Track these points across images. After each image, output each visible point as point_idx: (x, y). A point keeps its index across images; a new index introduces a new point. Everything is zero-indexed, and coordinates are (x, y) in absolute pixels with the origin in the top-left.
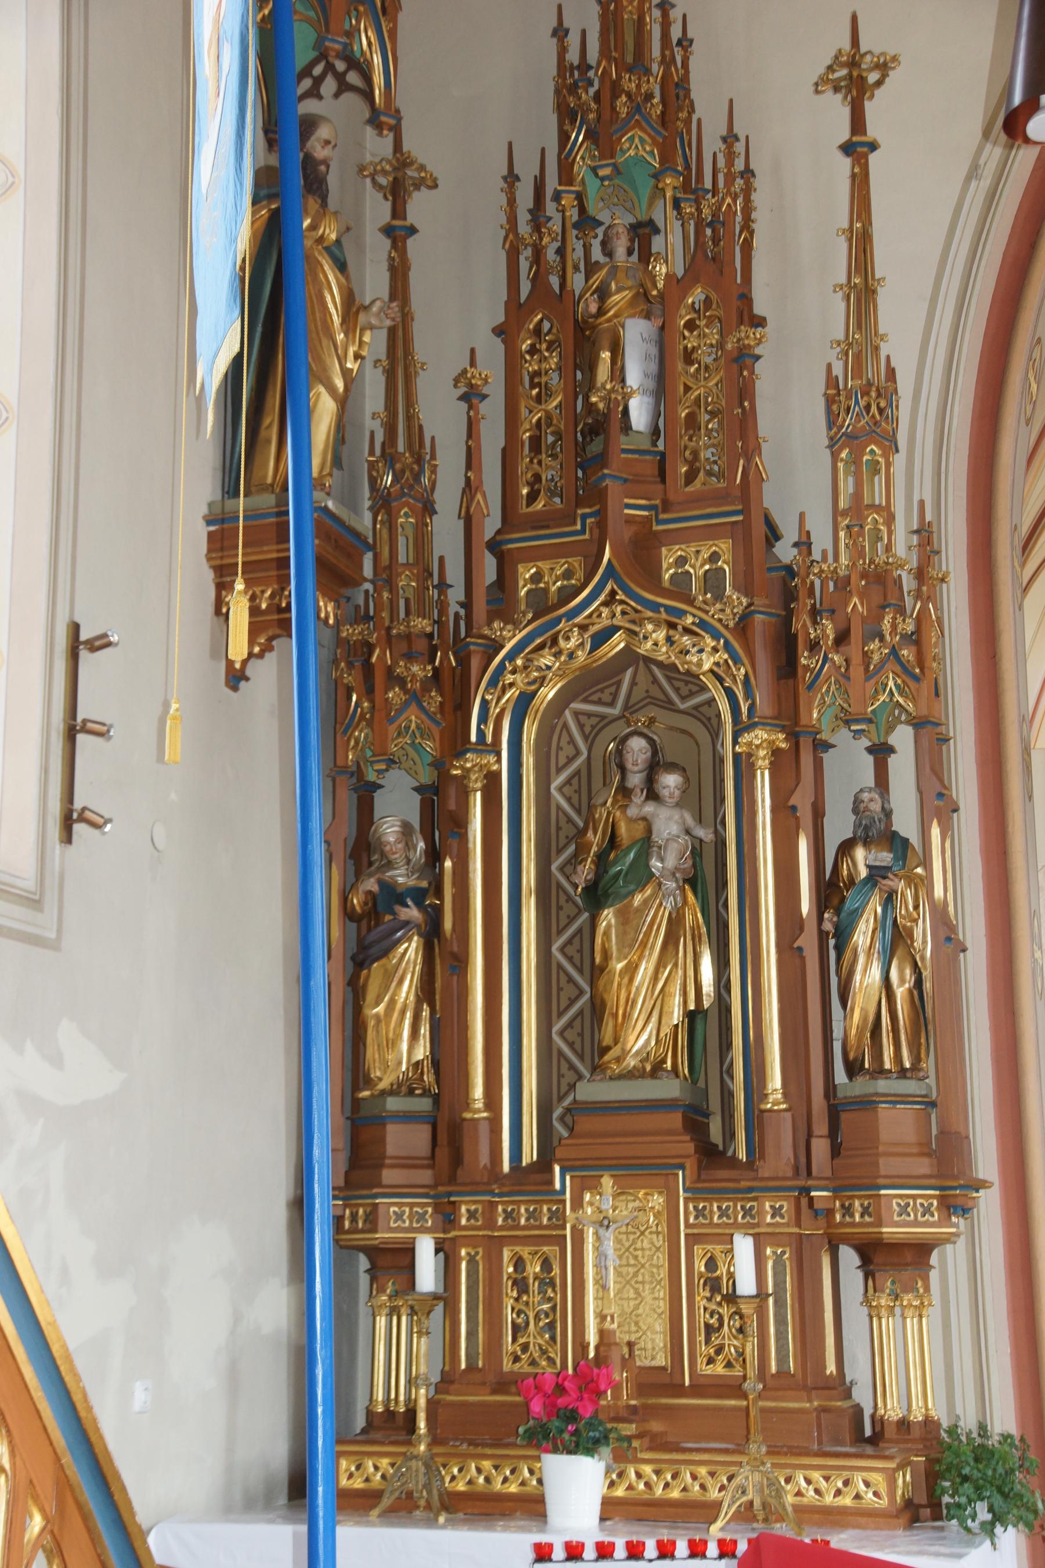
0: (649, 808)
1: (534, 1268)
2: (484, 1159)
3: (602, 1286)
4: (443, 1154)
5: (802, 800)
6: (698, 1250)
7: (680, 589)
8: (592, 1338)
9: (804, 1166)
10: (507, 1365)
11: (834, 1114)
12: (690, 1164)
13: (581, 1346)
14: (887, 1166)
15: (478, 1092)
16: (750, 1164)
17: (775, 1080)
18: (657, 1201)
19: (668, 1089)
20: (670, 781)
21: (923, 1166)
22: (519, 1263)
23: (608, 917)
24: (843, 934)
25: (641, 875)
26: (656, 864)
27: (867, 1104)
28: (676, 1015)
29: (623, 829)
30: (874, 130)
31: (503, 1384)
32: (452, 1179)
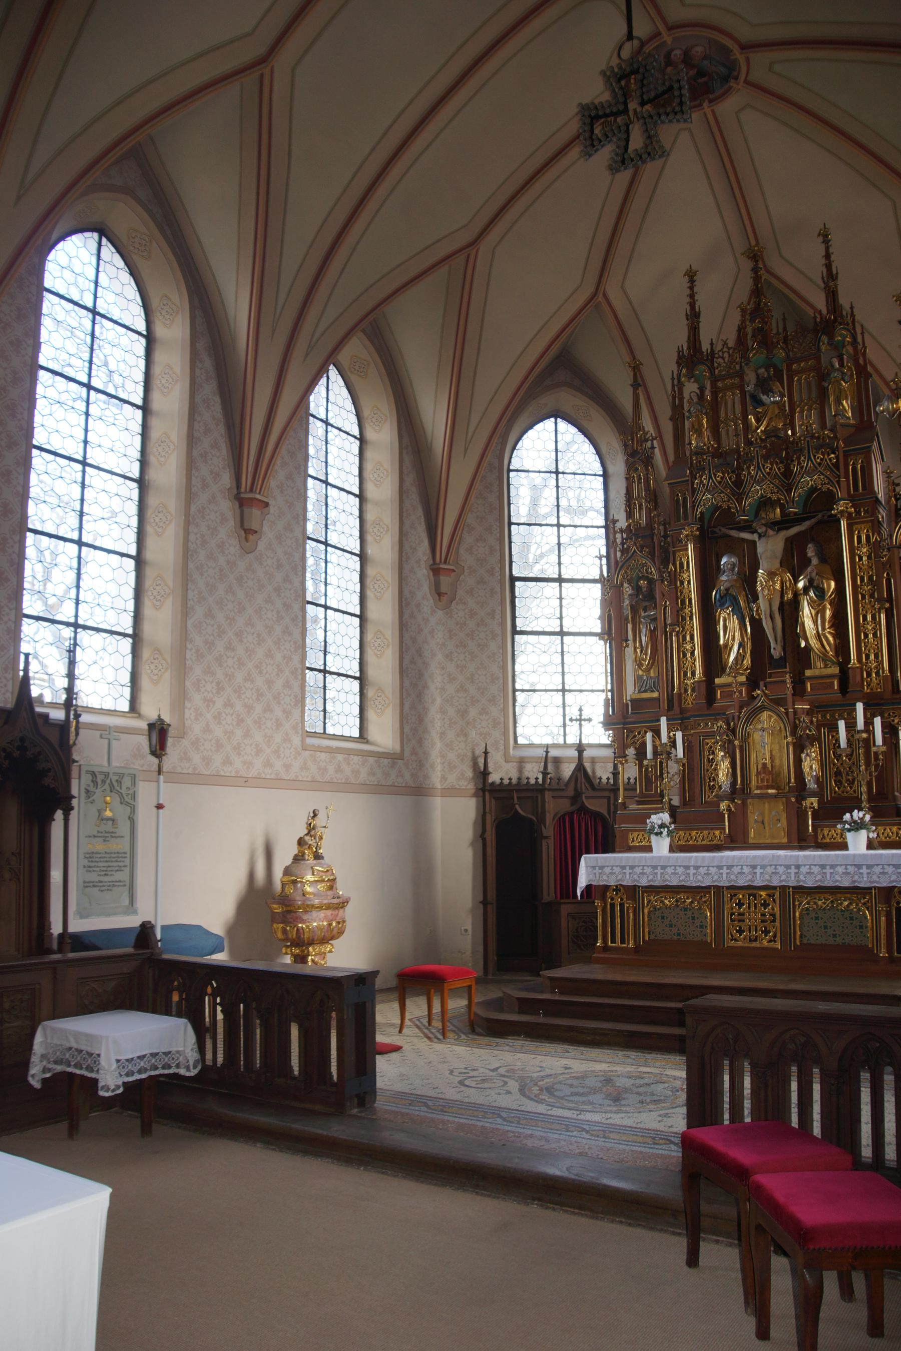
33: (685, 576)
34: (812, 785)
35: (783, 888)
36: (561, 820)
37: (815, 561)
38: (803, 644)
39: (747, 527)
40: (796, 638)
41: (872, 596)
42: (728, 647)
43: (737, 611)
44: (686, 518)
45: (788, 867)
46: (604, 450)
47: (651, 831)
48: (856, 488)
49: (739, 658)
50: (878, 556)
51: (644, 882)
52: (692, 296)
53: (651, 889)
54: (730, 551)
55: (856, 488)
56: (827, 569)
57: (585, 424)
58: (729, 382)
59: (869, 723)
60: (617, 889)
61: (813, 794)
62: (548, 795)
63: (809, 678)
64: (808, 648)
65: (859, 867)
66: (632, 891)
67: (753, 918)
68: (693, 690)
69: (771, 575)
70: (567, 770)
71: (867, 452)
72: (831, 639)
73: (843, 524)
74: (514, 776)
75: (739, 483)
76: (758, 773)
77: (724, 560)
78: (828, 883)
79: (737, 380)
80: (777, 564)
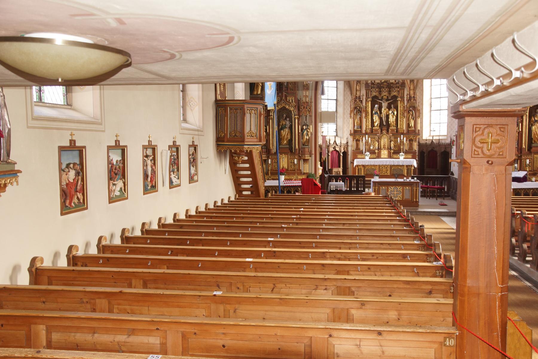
0: (286, 121)
1: (276, 161)
2: (272, 152)
4: (268, 152)
6: (290, 160)
7: (289, 102)
10: (274, 169)
12: (290, 153)
14: (306, 153)
15: (271, 146)
17: (297, 146)
20: (288, 119)
22: (275, 161)
23: (282, 131)
24: (303, 133)
25: (286, 128)
28: (288, 140)
31: (274, 170)
32: (269, 154)
34: (392, 148)
35: (390, 165)
36: (332, 152)
37: (393, 108)
38: (390, 123)
39: (381, 100)
41: (402, 115)
42: (376, 122)
43: (378, 115)
44: (368, 96)
45: (392, 162)
47: (366, 155)
48: (401, 96)
49: (378, 124)
50: (404, 108)
53: (368, 165)
54: (377, 104)
55: (401, 96)
59: (403, 138)
60: (360, 166)
61: (393, 150)
62: (330, 147)
63: (391, 129)
64: (391, 124)
65: (403, 162)
66: (363, 166)
67: (384, 170)
68: (368, 129)
69: (385, 110)
71: (404, 89)
72: (395, 122)
73: (399, 102)
75: (380, 91)
76: (383, 146)
77: (376, 106)
80: (386, 108)
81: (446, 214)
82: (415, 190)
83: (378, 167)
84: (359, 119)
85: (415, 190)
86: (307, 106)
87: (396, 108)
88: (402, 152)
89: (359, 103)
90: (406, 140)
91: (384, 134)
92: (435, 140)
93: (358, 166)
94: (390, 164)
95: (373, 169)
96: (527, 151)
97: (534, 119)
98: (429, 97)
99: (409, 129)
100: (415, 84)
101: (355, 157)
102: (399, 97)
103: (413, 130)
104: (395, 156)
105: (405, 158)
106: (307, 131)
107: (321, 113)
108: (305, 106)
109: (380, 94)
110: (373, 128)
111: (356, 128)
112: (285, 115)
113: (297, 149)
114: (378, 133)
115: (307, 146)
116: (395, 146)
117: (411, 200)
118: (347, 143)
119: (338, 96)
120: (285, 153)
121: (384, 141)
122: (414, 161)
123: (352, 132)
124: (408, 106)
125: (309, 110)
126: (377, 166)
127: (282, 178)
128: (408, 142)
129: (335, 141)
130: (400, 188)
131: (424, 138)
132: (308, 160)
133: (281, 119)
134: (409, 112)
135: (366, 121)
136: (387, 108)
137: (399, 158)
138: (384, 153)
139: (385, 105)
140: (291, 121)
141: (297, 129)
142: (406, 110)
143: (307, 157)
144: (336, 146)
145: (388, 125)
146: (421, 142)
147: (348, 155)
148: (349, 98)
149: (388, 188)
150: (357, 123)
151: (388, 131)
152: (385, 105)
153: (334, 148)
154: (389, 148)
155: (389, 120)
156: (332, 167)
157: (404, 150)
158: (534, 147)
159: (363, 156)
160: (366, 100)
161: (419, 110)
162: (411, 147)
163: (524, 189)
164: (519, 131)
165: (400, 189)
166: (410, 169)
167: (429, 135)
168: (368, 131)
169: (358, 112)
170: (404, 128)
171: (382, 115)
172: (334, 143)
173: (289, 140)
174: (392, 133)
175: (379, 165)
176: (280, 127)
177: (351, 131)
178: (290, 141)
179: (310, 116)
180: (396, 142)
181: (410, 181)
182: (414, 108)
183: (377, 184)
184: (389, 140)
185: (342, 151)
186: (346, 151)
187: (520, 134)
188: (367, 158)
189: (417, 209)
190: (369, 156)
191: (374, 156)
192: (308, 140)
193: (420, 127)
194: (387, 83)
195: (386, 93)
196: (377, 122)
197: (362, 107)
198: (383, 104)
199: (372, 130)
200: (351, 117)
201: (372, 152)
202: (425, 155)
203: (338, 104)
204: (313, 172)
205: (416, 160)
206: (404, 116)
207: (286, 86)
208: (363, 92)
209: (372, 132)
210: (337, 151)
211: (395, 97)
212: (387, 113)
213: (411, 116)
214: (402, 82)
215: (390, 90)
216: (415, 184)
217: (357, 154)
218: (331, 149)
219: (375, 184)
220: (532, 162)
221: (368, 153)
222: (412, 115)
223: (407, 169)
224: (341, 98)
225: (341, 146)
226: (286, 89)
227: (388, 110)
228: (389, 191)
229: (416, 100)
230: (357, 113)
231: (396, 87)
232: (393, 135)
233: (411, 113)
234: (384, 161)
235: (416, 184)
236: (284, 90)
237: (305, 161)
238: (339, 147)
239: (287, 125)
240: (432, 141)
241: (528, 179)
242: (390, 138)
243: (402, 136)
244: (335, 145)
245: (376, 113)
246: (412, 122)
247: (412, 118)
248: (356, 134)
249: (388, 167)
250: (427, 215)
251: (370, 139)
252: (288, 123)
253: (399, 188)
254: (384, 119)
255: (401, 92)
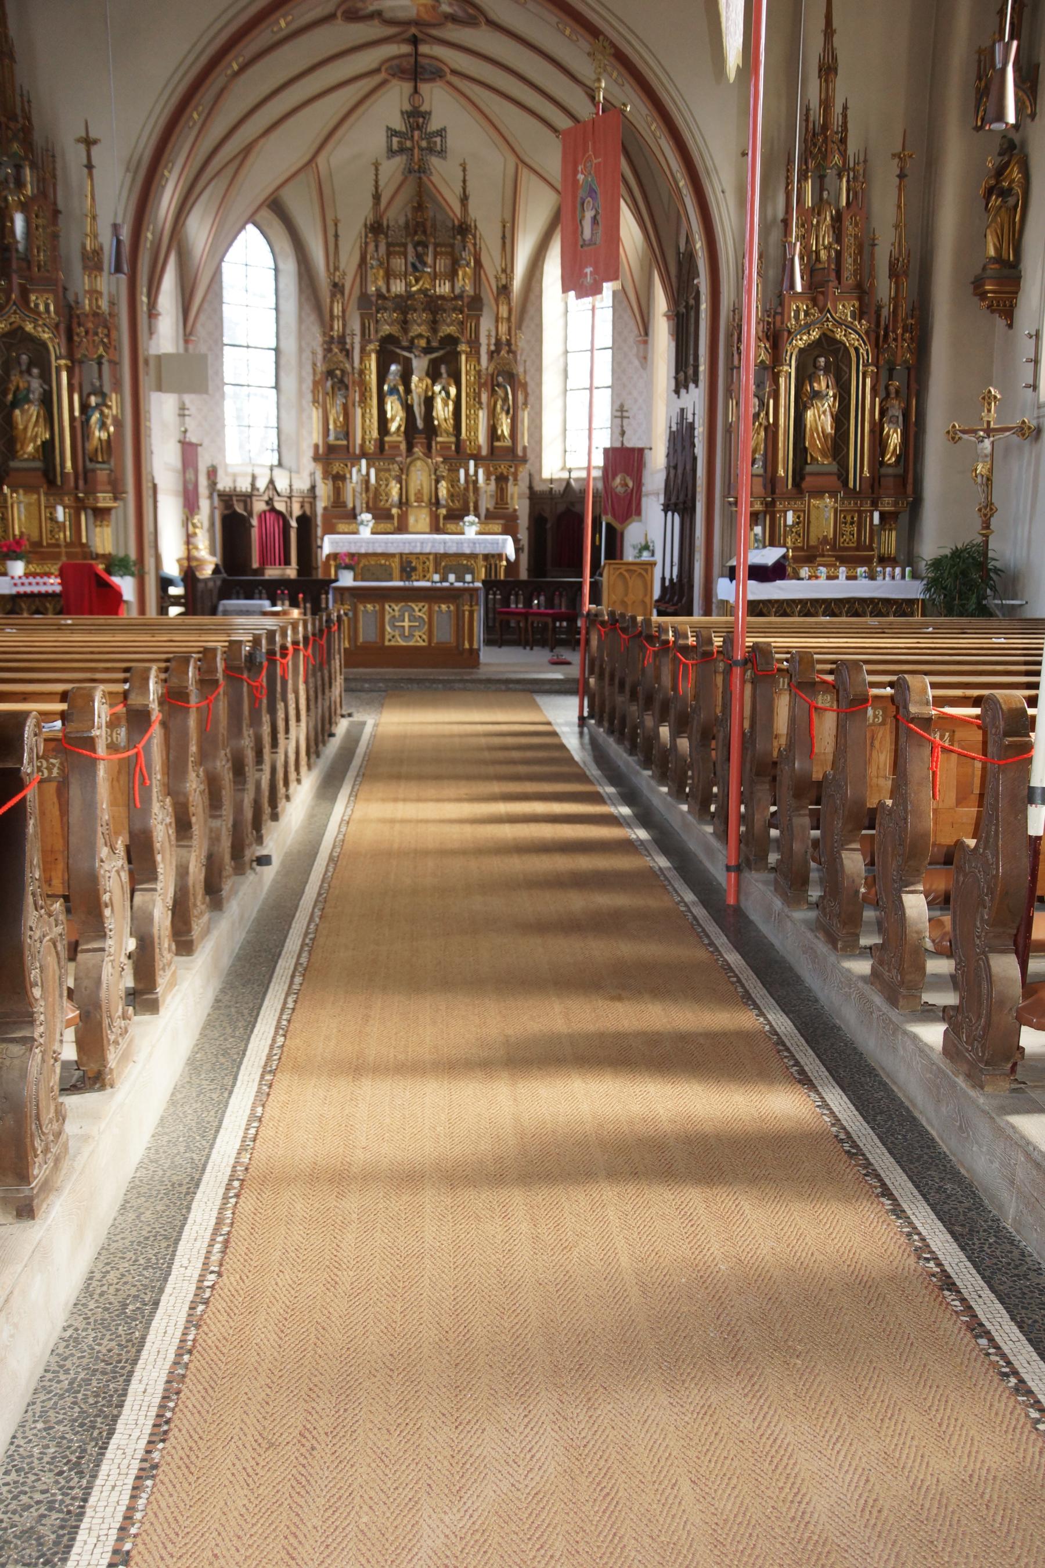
0: (29, 379)
3: (19, 519)
5: (76, 382)
8: (17, 532)
9: (77, 487)
11: (86, 472)
12: (45, 486)
13: (14, 536)
14: (99, 488)
16: (61, 487)
17: (69, 464)
18: (35, 497)
19: (38, 464)
20: (35, 371)
21: (109, 488)
23: (17, 412)
24: (88, 420)
26: (31, 396)
27: (94, 471)
29: (21, 385)
30: (94, 162)
33: (367, 372)
34: (443, 502)
35: (436, 555)
36: (262, 516)
37: (445, 375)
38: (436, 423)
39: (409, 349)
40: (432, 419)
42: (393, 419)
43: (400, 399)
46: (277, 250)
47: (362, 523)
49: (400, 426)
50: (480, 378)
51: (363, 551)
52: (377, 181)
53: (366, 555)
54: (397, 362)
56: (452, 382)
57: (265, 228)
58: (397, 249)
61: (444, 507)
62: (254, 498)
64: (439, 425)
65: (474, 543)
69: (421, 380)
70: (262, 484)
72: (452, 421)
73: (463, 357)
74: (232, 486)
75: (405, 322)
78: (460, 551)
79: (402, 249)
80: (424, 374)
81: (557, 687)
82: (467, 613)
83: (397, 559)
84: (340, 409)
85: (467, 613)
86: (97, 327)
87: (456, 377)
88: (472, 513)
89: (341, 357)
90: (488, 479)
91: (416, 456)
92: (577, 480)
93: (334, 556)
94: (434, 551)
95: (381, 565)
96: (790, 486)
97: (812, 387)
98: (560, 349)
99: (497, 444)
100: (514, 304)
101: (330, 530)
102: (463, 340)
103: (507, 447)
104: (451, 527)
105: (480, 533)
106: (102, 413)
107: (159, 358)
108: (90, 325)
109: (405, 331)
110: (387, 439)
111: (332, 437)
112: (24, 357)
113: (68, 474)
114: (401, 455)
115: (103, 462)
116: (451, 496)
117: (457, 646)
118: (313, 488)
119: (282, 336)
120: (30, 489)
121: (420, 477)
122: (506, 540)
123: (321, 451)
124: (491, 370)
125: (105, 340)
126: (393, 555)
127: (18, 568)
128: (493, 483)
129: (271, 482)
130: (419, 610)
131: (546, 474)
132: (108, 510)
133: (13, 372)
134: (493, 392)
135: (363, 416)
136: (428, 374)
137: (463, 533)
138: (419, 518)
139: (420, 364)
140: (45, 377)
141: (67, 405)
142: (486, 383)
143: (104, 500)
144: (276, 498)
145: (431, 429)
146: (539, 487)
147: (317, 526)
148: (316, 340)
149: (383, 609)
150: (335, 423)
151: (429, 447)
152: (420, 364)
153: (267, 503)
154: (433, 500)
155: (434, 414)
156: (264, 562)
157: (483, 512)
158: (811, 474)
159: (352, 527)
160: (363, 350)
161: (525, 386)
162: (502, 499)
163: (777, 601)
164: (765, 423)
165: (420, 610)
166: (496, 566)
167: (560, 465)
168: (371, 447)
169: (339, 389)
170: (482, 438)
171: (412, 399)
172: (267, 488)
173: (43, 443)
174: (442, 456)
175: (401, 554)
176: (10, 397)
177: (316, 447)
178: (48, 449)
179: (110, 361)
180: (454, 482)
181: (452, 584)
182: (511, 377)
183: (347, 595)
184: (433, 477)
185: (297, 511)
186: (308, 512)
187: (770, 434)
188: (365, 532)
189: (471, 673)
190: (371, 524)
191: (389, 527)
192: (104, 444)
193: (530, 436)
194: (426, 295)
195: (423, 327)
196: (398, 419)
197: (348, 366)
198: (415, 363)
199: (381, 444)
200: (315, 401)
201: (381, 515)
202: (549, 526)
203: (283, 362)
204: (133, 555)
205: (516, 541)
206: (480, 403)
207: (23, 256)
208: (355, 326)
209: (381, 452)
210: (279, 513)
211: (451, 341)
212: (426, 391)
213: (499, 403)
214: (472, 293)
215: (434, 317)
216: (467, 596)
217: (334, 521)
218: (259, 506)
219: (342, 595)
220: (804, 521)
221: (366, 517)
222: (505, 399)
223: (486, 567)
224: (290, 346)
225: (290, 498)
226: (24, 265)
227: (429, 382)
228: (387, 618)
229: (514, 353)
230: (336, 389)
231: (454, 309)
232: (446, 460)
233: (500, 392)
234: (416, 541)
235: (471, 596)
236: (14, 266)
237: (101, 514)
238: (285, 499)
239: (33, 393)
240: (568, 483)
241: (789, 570)
242: (436, 470)
243: (472, 463)
244: (271, 493)
245: (393, 390)
246: (504, 421)
247: (502, 409)
248: (332, 456)
249: (428, 559)
250: (496, 691)
251: (373, 471)
252: (36, 384)
253: (417, 609)
254: (418, 411)
255: (470, 324)
